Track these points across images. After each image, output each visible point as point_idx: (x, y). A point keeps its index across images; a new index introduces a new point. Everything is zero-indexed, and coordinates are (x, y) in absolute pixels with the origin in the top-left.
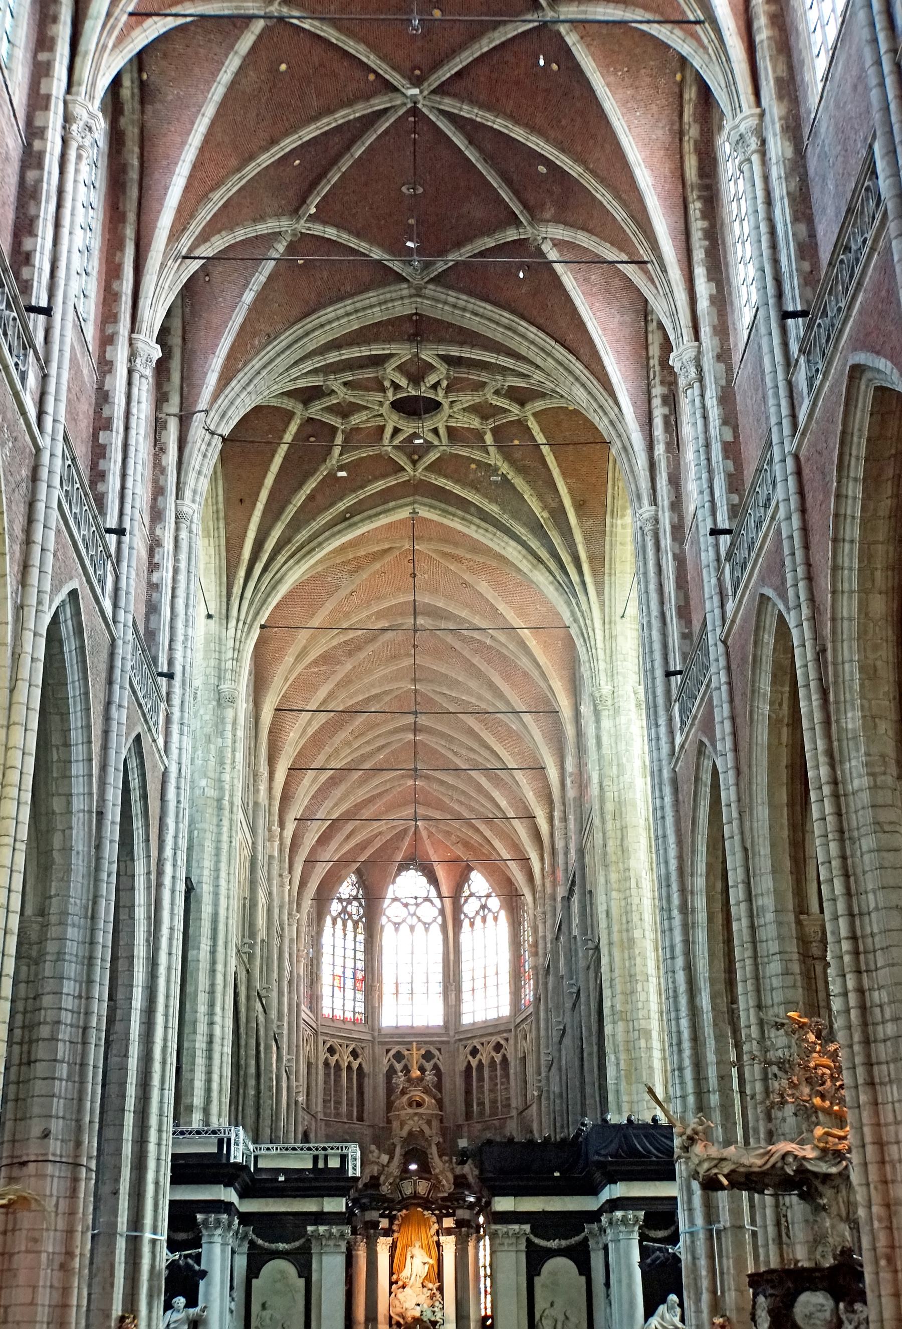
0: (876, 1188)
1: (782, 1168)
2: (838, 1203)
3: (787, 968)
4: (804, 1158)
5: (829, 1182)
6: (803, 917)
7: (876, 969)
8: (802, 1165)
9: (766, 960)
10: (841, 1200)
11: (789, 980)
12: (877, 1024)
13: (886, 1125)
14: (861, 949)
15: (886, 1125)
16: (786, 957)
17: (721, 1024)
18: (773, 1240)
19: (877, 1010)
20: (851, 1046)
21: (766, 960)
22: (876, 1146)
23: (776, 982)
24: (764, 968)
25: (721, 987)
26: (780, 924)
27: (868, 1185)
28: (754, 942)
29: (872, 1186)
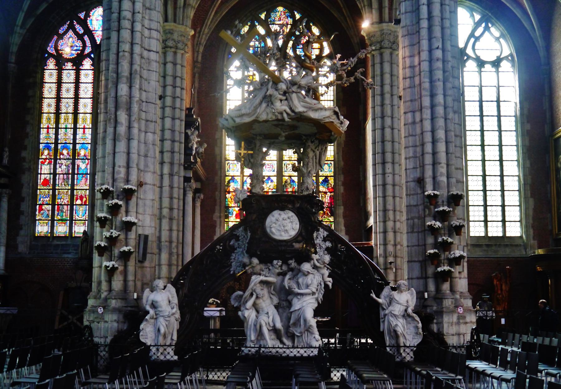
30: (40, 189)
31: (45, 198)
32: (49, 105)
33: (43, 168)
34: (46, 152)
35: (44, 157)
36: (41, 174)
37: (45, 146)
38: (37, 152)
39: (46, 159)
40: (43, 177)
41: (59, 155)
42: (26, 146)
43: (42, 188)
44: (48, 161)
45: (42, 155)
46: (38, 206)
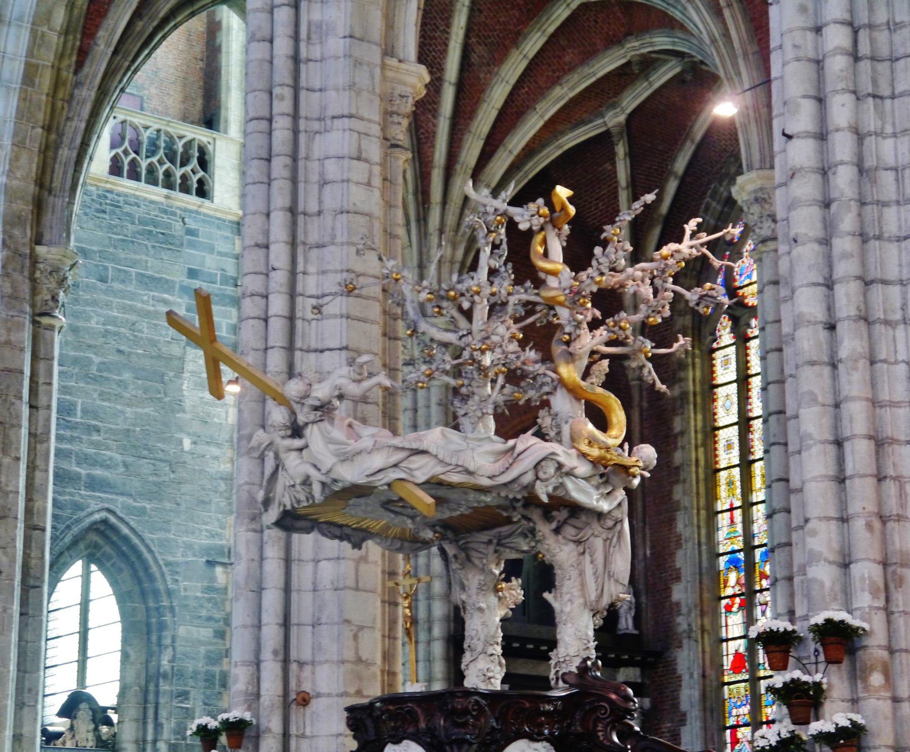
0: (869, 527)
1: (530, 487)
2: (582, 573)
3: (360, 150)
4: (570, 474)
5: (569, 531)
6: (393, 62)
7: (893, 97)
8: (562, 485)
9: (316, 126)
10: (589, 570)
11: (359, 171)
12: (885, 204)
13: (893, 404)
14: (864, 49)
15: (893, 404)
16: (359, 125)
17: (17, 276)
18: (275, 653)
19: (887, 178)
20: (826, 242)
21: (316, 126)
22: (873, 443)
23: (332, 170)
24: (311, 140)
25: (25, 208)
26: (357, 63)
27: (844, 520)
28: (296, 88)
29: (859, 525)
30: (729, 684)
31: (740, 706)
32: (729, 446)
33: (730, 622)
34: (733, 577)
35: (729, 592)
36: (727, 640)
37: (730, 562)
38: (715, 579)
39: (734, 596)
40: (732, 647)
41: (758, 579)
42: (680, 569)
43: (733, 679)
44: (737, 600)
45: (725, 587)
46: (728, 732)
